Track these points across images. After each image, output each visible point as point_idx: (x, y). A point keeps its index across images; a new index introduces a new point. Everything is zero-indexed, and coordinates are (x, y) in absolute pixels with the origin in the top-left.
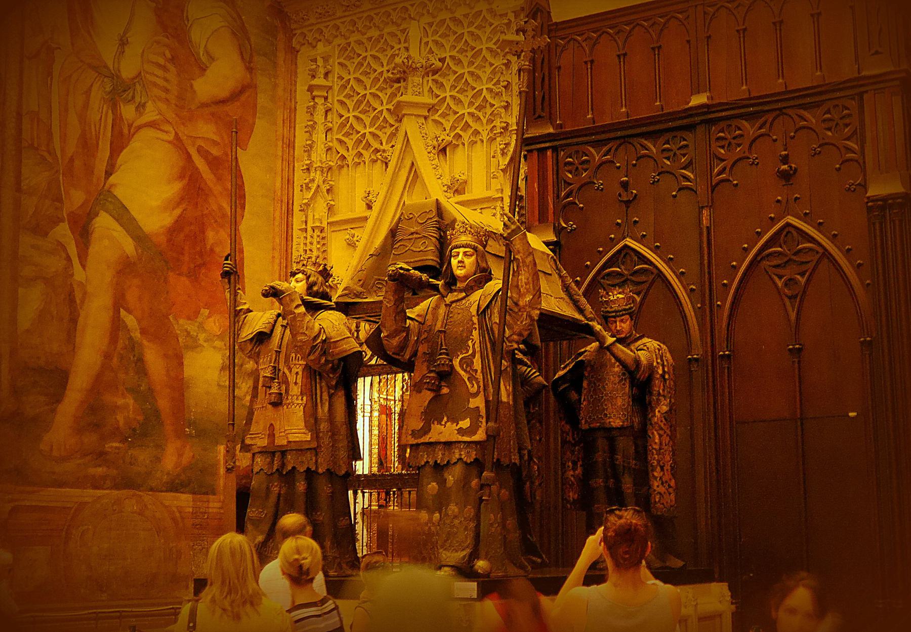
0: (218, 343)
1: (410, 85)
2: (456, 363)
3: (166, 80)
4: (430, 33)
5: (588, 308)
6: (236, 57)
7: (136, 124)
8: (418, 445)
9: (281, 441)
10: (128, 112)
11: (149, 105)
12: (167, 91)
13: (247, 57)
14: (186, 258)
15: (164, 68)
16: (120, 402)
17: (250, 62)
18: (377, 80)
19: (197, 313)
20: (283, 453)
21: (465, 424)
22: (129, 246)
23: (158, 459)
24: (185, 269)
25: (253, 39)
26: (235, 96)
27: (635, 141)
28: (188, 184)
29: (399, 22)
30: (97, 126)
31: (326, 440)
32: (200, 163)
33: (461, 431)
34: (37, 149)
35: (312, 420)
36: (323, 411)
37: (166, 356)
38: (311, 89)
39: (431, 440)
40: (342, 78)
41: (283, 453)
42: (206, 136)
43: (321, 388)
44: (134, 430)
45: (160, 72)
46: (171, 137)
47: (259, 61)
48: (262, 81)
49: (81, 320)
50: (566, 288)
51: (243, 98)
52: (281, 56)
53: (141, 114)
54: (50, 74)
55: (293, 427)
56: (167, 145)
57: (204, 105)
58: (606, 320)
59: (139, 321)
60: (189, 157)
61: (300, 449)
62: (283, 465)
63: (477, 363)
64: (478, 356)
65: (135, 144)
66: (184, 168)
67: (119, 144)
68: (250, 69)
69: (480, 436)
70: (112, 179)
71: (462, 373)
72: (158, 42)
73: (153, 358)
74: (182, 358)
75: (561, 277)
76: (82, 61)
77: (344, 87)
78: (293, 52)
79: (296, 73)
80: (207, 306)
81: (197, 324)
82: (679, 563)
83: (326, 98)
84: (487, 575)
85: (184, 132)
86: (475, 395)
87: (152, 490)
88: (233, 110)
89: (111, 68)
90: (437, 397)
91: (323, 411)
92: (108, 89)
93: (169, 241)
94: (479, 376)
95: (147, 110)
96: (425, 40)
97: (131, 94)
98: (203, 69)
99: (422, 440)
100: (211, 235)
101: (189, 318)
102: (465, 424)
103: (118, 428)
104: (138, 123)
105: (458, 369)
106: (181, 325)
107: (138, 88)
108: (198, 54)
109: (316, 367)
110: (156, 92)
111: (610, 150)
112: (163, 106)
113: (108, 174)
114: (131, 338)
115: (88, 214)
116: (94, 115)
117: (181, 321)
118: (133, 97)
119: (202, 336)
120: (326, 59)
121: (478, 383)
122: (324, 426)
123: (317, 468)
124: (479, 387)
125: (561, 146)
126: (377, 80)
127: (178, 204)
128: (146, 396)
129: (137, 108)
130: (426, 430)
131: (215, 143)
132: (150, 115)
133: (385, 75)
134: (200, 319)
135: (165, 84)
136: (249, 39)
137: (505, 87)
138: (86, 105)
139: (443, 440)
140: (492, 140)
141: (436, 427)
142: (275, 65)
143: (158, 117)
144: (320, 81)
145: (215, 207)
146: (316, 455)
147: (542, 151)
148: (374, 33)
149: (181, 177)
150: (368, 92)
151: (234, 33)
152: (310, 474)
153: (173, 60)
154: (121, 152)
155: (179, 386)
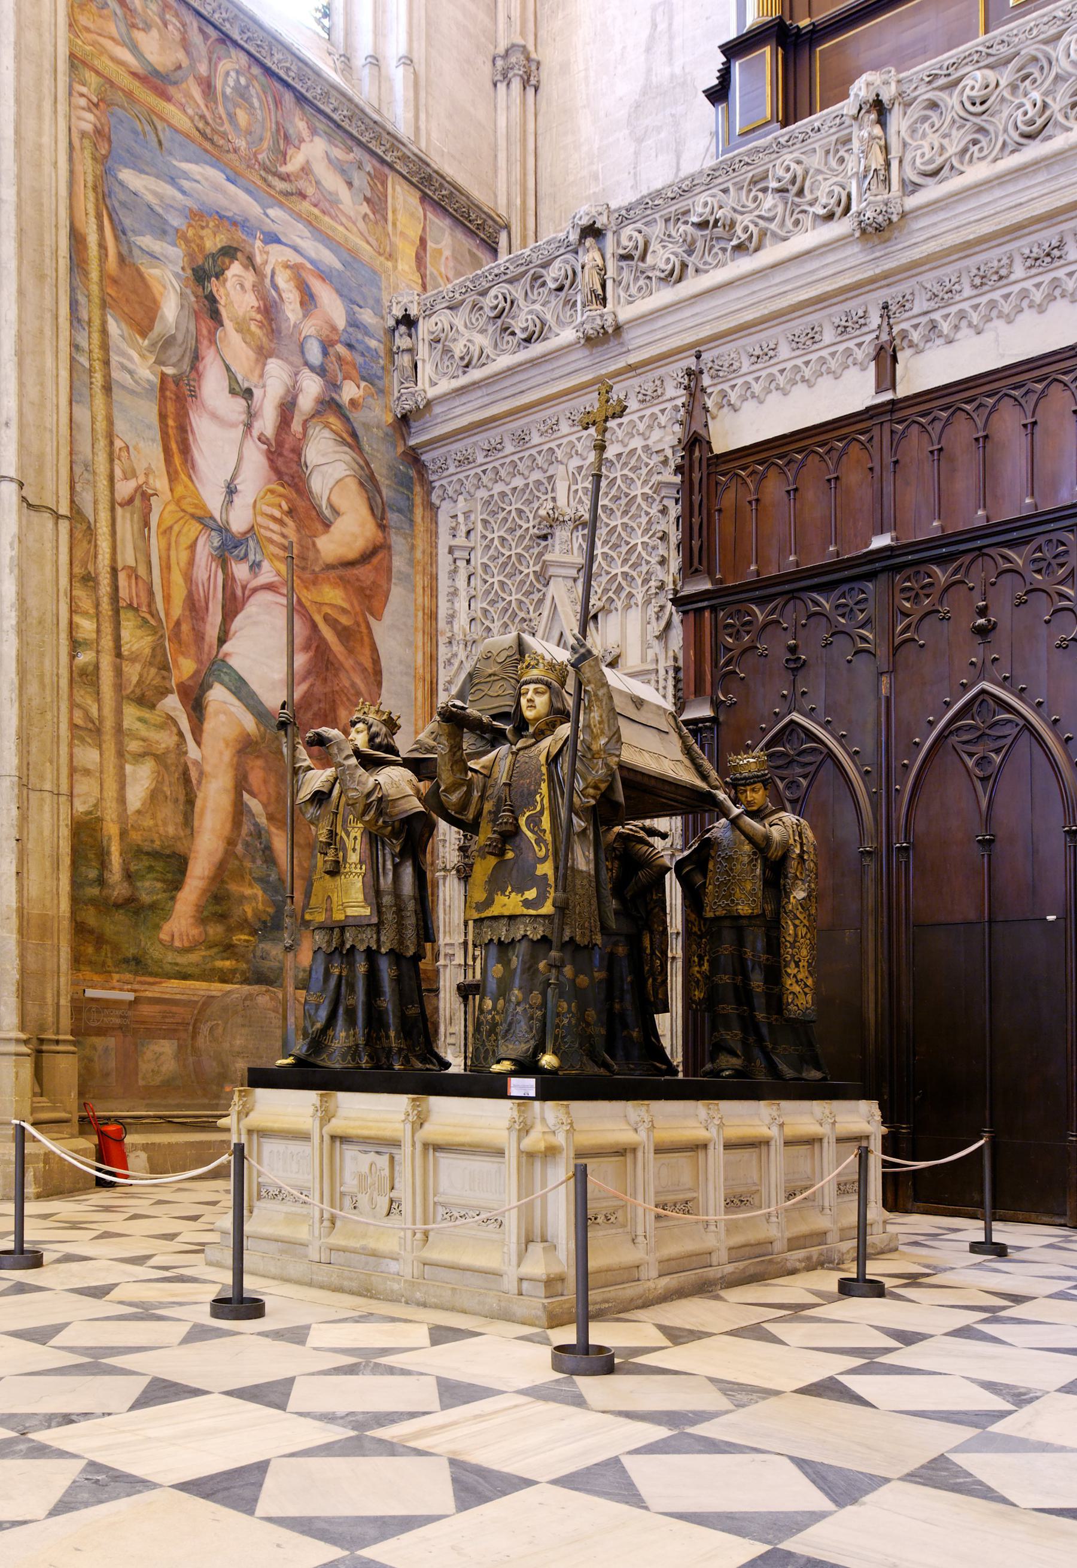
1: (557, 542)
2: (522, 821)
3: (284, 536)
4: (579, 479)
5: (714, 774)
6: (364, 511)
7: (250, 586)
8: (482, 920)
9: (339, 916)
10: (241, 571)
11: (266, 565)
13: (379, 514)
17: (382, 519)
18: (522, 537)
20: (342, 929)
21: (531, 894)
22: (249, 723)
25: (385, 491)
26: (365, 558)
27: (805, 595)
28: (315, 656)
29: (545, 466)
31: (389, 916)
33: (527, 903)
34: (136, 610)
35: (374, 894)
36: (386, 882)
38: (451, 551)
39: (496, 914)
40: (484, 537)
41: (342, 929)
42: (334, 602)
43: (384, 855)
45: (275, 527)
47: (393, 517)
48: (398, 542)
49: (199, 803)
50: (688, 751)
51: (375, 560)
52: (419, 512)
53: (256, 576)
55: (351, 898)
57: (330, 567)
58: (736, 786)
61: (359, 925)
62: (343, 943)
63: (546, 822)
64: (546, 813)
65: (252, 608)
66: (309, 639)
67: (232, 607)
68: (382, 527)
69: (547, 909)
71: (529, 834)
72: (272, 492)
75: (681, 737)
76: (183, 511)
77: (488, 547)
78: (432, 509)
79: (437, 533)
82: (815, 1074)
83: (468, 561)
84: (553, 1072)
85: (307, 596)
86: (543, 860)
88: (364, 573)
89: (218, 519)
90: (502, 863)
91: (386, 882)
92: (216, 544)
94: (548, 837)
96: (574, 488)
98: (327, 525)
99: (483, 915)
102: (531, 894)
103: (246, 920)
104: (254, 583)
105: (524, 829)
107: (251, 543)
108: (320, 507)
109: (373, 830)
110: (273, 549)
111: (776, 607)
115: (201, 685)
116: (201, 573)
118: (246, 555)
120: (467, 514)
121: (546, 846)
122: (387, 900)
123: (379, 947)
124: (547, 850)
125: (721, 604)
126: (522, 537)
129: (251, 567)
130: (489, 902)
131: (344, 611)
132: (268, 574)
133: (531, 531)
136: (380, 493)
137: (661, 539)
139: (507, 913)
140: (647, 602)
141: (500, 899)
142: (412, 522)
143: (276, 579)
144: (461, 540)
146: (378, 933)
147: (699, 611)
148: (518, 482)
150: (513, 552)
151: (361, 484)
152: (371, 955)
153: (291, 512)
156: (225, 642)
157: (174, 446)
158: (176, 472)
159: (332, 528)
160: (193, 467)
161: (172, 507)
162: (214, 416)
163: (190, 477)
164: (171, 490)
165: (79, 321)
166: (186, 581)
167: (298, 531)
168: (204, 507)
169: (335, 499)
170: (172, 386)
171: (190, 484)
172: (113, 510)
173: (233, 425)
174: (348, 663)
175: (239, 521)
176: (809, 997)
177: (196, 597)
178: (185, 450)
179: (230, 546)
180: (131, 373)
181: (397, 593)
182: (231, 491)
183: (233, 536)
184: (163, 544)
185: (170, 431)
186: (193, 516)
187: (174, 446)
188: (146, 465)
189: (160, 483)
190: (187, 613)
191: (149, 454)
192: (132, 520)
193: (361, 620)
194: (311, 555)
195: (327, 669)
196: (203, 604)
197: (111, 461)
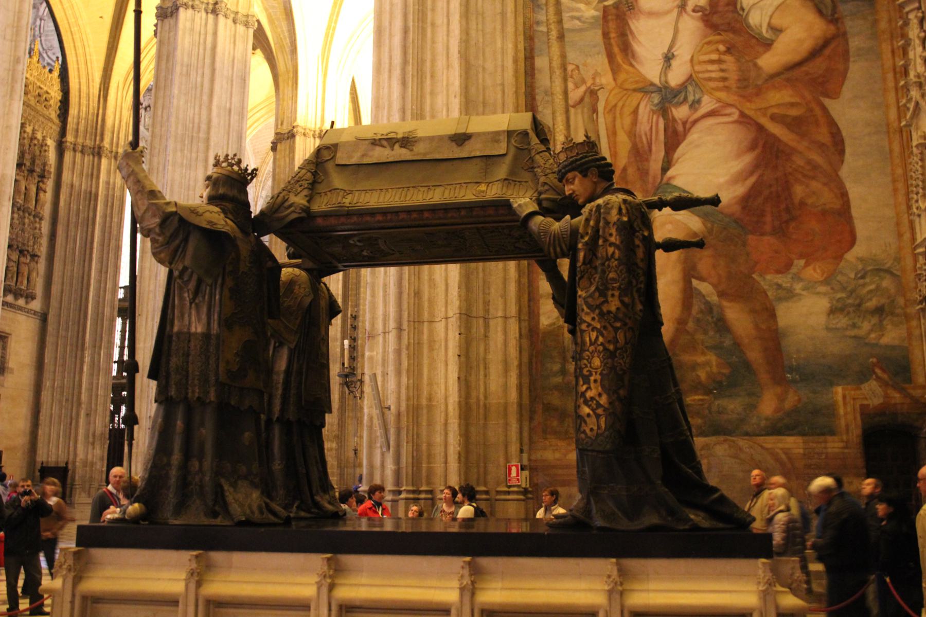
0: (822, 289)
3: (722, 70)
7: (691, 120)
10: (680, 112)
11: (706, 99)
12: (724, 79)
14: (768, 218)
15: (719, 61)
16: (701, 359)
19: (789, 265)
23: (753, 407)
24: (768, 228)
26: (814, 54)
30: (648, 134)
32: (776, 129)
37: (753, 311)
44: (720, 383)
45: (711, 67)
46: (736, 116)
51: (827, 52)
53: (696, 110)
54: (595, 110)
56: (732, 126)
59: (714, 286)
60: (760, 128)
70: (670, 173)
72: (709, 43)
73: (737, 317)
74: (774, 310)
76: (626, 90)
80: (801, 256)
81: (790, 276)
85: (750, 109)
87: (747, 434)
88: (818, 66)
92: (656, 101)
93: (744, 208)
95: (703, 103)
97: (682, 98)
98: (768, 45)
100: (799, 191)
101: (778, 272)
106: (768, 281)
107: (690, 88)
108: (760, 34)
110: (712, 84)
112: (722, 95)
113: (665, 170)
114: (707, 303)
117: (768, 277)
118: (685, 99)
119: (798, 287)
127: (751, 173)
128: (732, 352)
129: (691, 106)
131: (792, 105)
134: (794, 270)
135: (722, 74)
138: (635, 122)
143: (717, 105)
145: (799, 161)
149: (752, 147)
153: (728, 51)
154: (677, 147)
155: (773, 339)
156: (668, 169)
157: (616, 50)
158: (619, 66)
159: (775, 45)
160: (634, 56)
161: (617, 91)
162: (651, 14)
163: (631, 65)
164: (615, 80)
165: (539, 6)
166: (629, 137)
167: (738, 60)
168: (645, 79)
169: (776, 22)
170: (614, 11)
171: (630, 69)
172: (567, 111)
173: (668, 12)
174: (802, 146)
175: (675, 78)
176: (602, 421)
177: (640, 145)
178: (626, 48)
179: (668, 97)
180: (578, 19)
181: (857, 70)
182: (668, 58)
183: (672, 89)
184: (610, 118)
185: (613, 41)
186: (635, 90)
187: (616, 50)
188: (592, 72)
189: (606, 79)
190: (633, 160)
191: (592, 63)
192: (583, 112)
193: (813, 105)
194: (753, 74)
195: (777, 157)
196: (646, 148)
197: (565, 80)
